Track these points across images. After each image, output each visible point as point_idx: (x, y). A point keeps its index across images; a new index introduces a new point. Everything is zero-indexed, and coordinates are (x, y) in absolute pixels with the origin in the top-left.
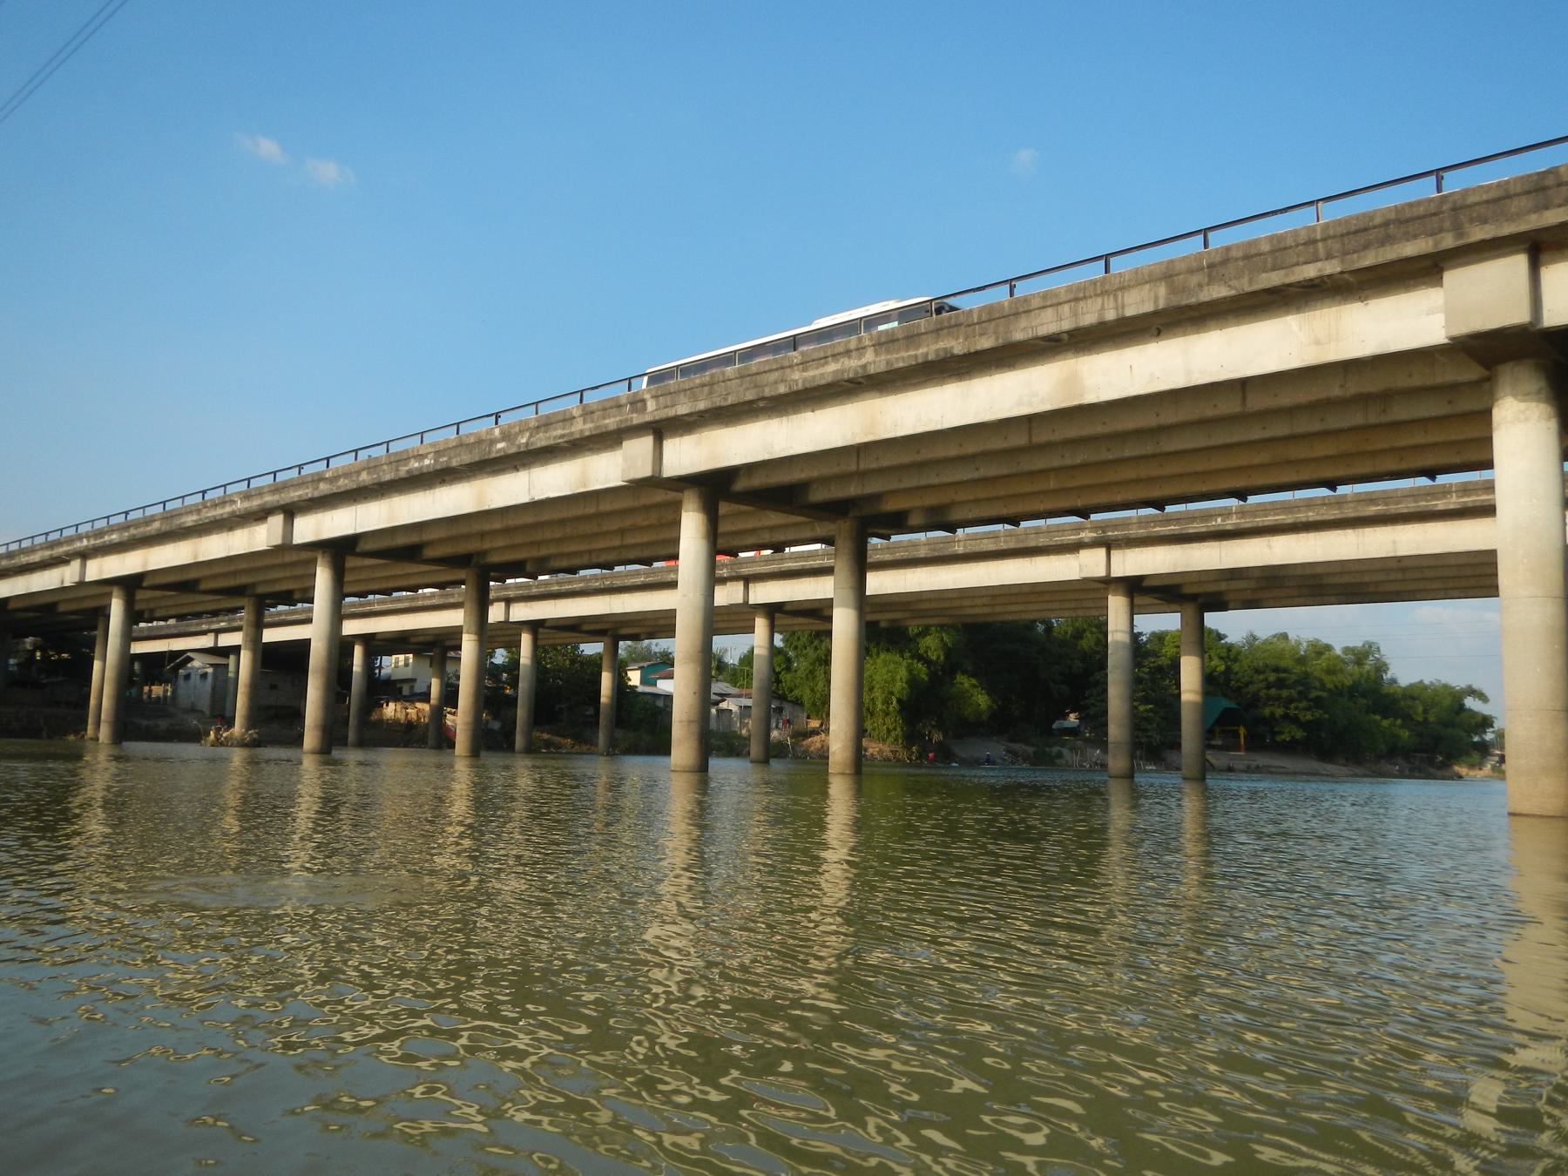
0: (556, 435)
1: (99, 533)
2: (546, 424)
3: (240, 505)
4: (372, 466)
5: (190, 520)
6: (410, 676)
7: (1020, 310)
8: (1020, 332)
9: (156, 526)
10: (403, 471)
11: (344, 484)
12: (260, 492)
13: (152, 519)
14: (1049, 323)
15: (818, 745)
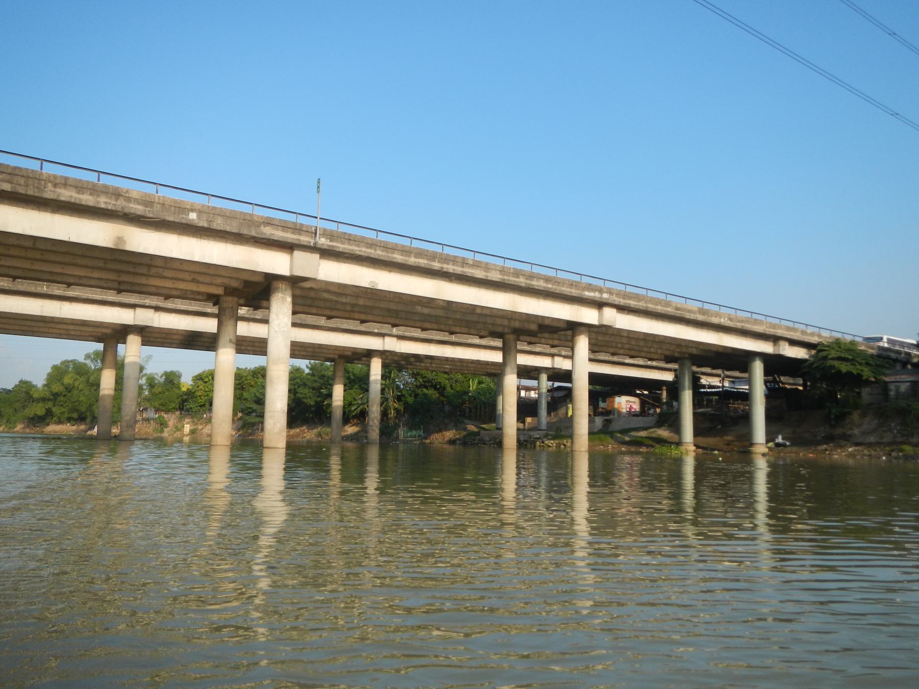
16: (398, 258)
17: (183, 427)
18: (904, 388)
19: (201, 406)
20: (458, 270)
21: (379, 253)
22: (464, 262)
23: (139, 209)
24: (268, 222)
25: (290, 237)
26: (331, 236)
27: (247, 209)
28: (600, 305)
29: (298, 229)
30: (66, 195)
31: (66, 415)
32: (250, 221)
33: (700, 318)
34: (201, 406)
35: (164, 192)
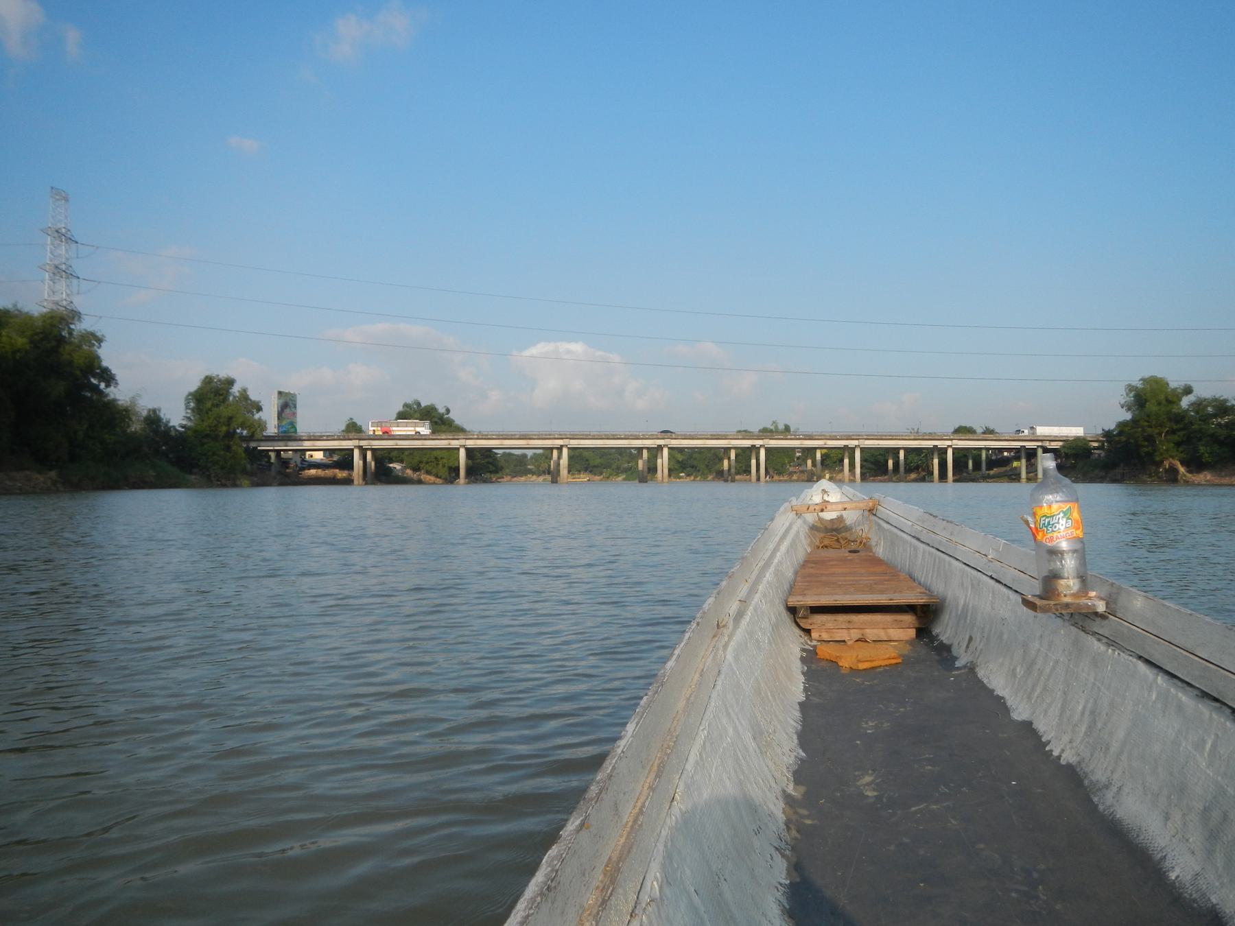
0: (655, 437)
1: (487, 435)
2: (653, 435)
3: (556, 436)
4: (605, 435)
5: (534, 437)
6: (291, 457)
7: (727, 435)
8: (728, 437)
9: (517, 437)
10: (616, 437)
11: (596, 437)
12: (566, 435)
13: (515, 435)
14: (731, 437)
15: (428, 479)
16: (884, 437)
17: (825, 475)
18: (1097, 455)
19: (834, 463)
20: (901, 438)
21: (879, 437)
22: (902, 436)
23: (828, 437)
24: (853, 435)
25: (858, 437)
26: (867, 435)
27: (848, 434)
28: (951, 440)
29: (859, 436)
30: (817, 437)
31: (744, 468)
32: (849, 436)
33: (995, 438)
34: (834, 463)
35: (834, 434)
